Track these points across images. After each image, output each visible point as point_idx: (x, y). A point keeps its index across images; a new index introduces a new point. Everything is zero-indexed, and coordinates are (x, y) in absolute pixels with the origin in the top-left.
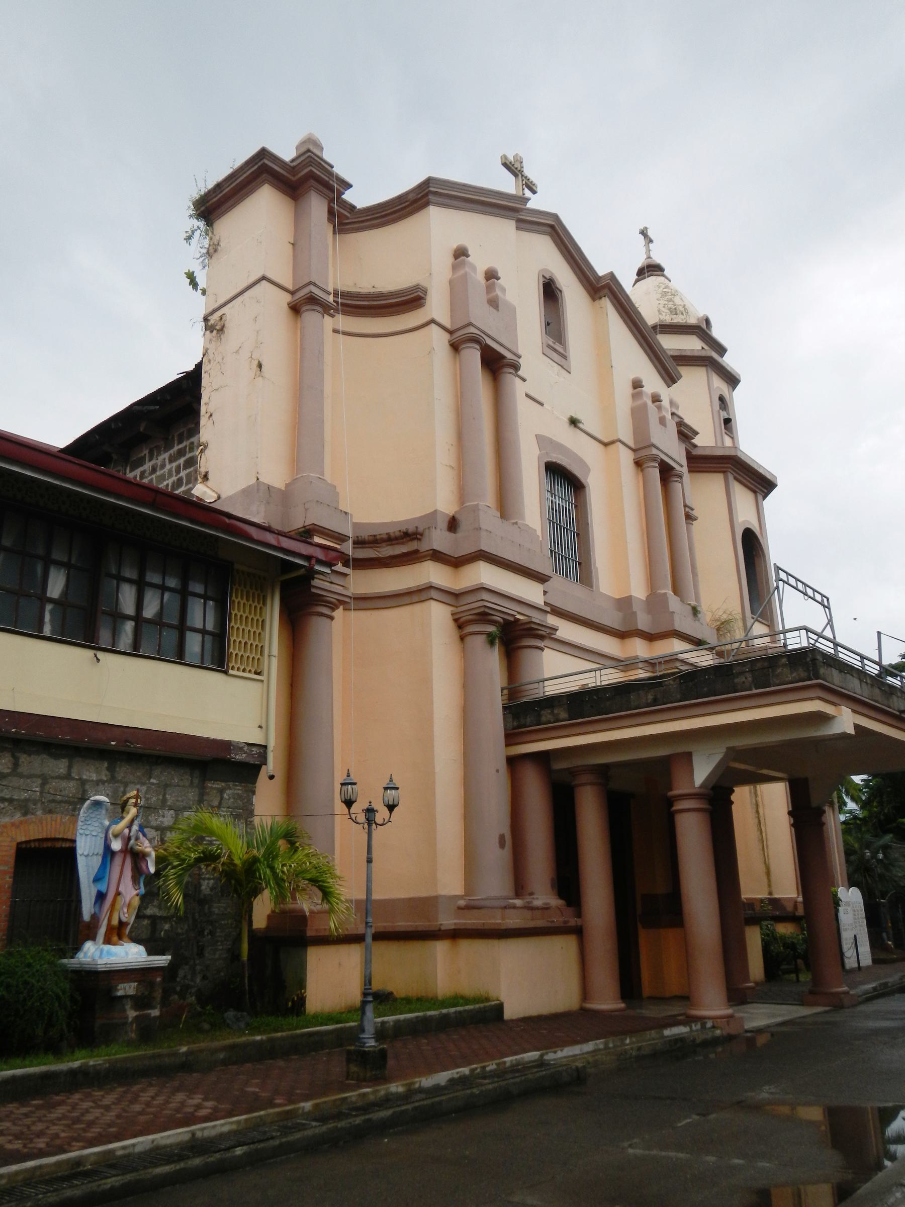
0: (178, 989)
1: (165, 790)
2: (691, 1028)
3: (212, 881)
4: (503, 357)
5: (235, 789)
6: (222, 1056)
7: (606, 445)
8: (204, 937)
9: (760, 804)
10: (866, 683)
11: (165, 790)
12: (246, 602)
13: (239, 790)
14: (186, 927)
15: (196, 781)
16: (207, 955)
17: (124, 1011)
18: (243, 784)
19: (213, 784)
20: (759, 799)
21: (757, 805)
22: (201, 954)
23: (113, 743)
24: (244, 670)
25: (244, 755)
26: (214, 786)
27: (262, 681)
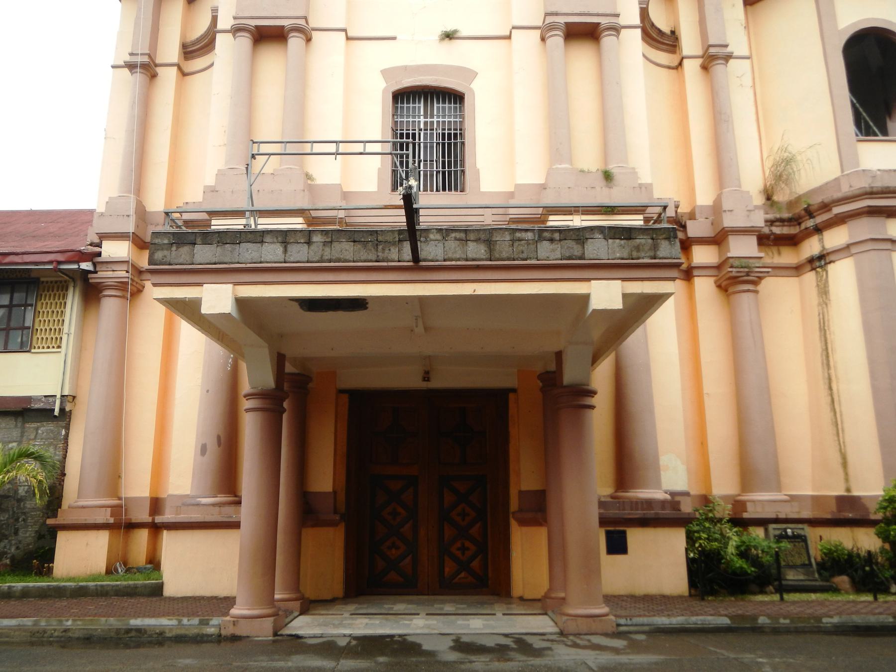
2: (180, 621)
3: (26, 487)
4: (283, 27)
5: (48, 426)
7: (509, 37)
9: (833, 378)
10: (309, 243)
12: (53, 302)
13: (51, 426)
15: (19, 424)
16: (20, 534)
18: (54, 423)
20: (832, 372)
21: (830, 379)
22: (16, 533)
24: (48, 347)
25: (42, 404)
27: (60, 352)
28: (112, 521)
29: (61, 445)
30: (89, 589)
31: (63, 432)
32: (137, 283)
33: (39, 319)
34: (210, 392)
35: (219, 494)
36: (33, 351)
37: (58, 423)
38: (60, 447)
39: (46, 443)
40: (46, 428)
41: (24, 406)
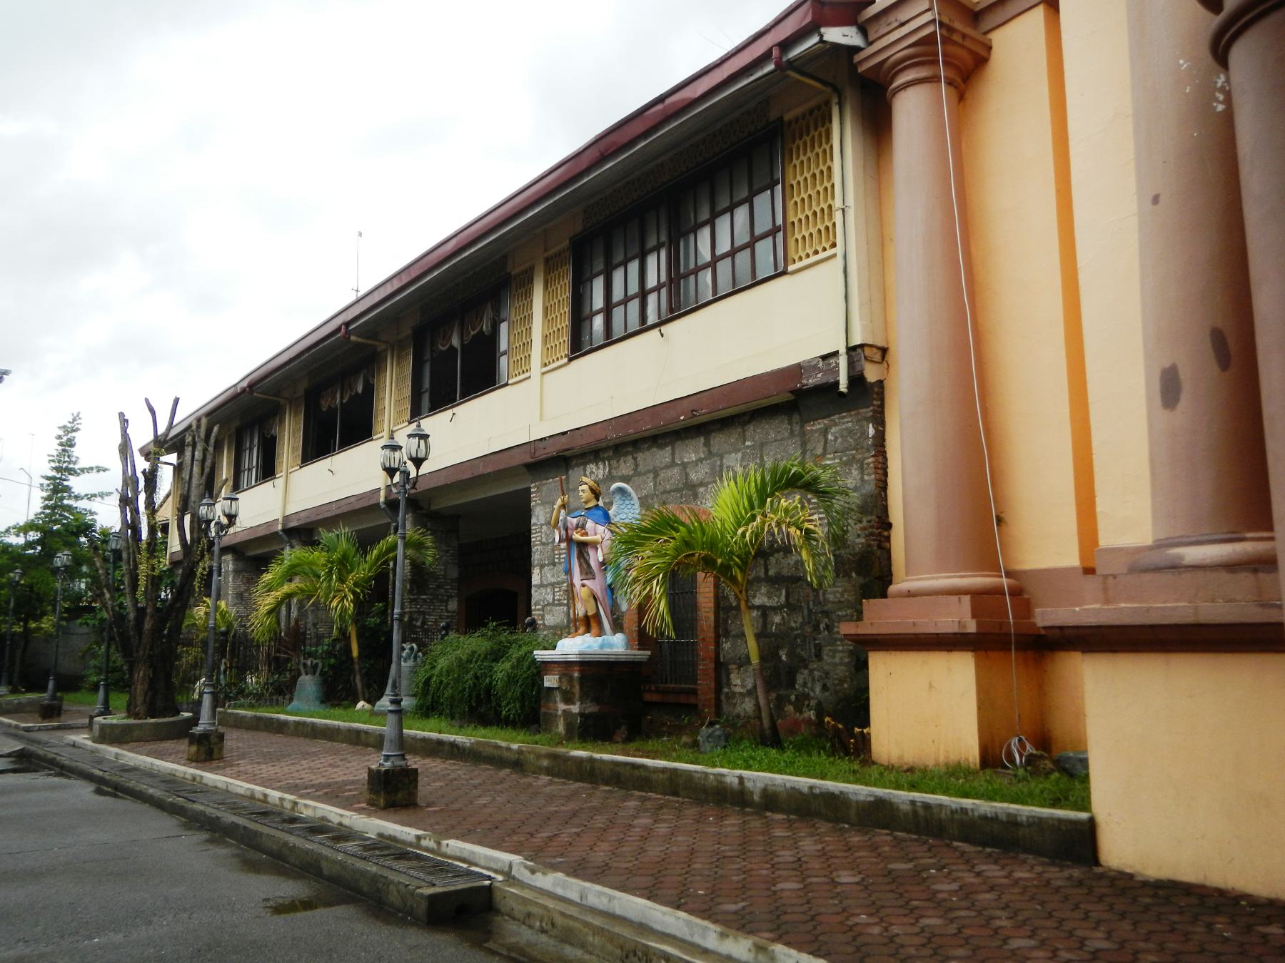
0: (793, 698)
1: (761, 450)
5: (843, 423)
6: (545, 763)
8: (820, 633)
11: (761, 450)
13: (847, 422)
14: (800, 620)
15: (797, 428)
16: (825, 657)
17: (556, 702)
18: (853, 413)
19: (813, 425)
22: (819, 656)
23: (682, 418)
24: (816, 252)
25: (819, 375)
26: (814, 428)
28: (972, 627)
29: (871, 460)
30: (898, 809)
31: (871, 431)
32: (964, 36)
33: (792, 202)
34: (1162, 198)
35: (1250, 530)
36: (791, 268)
37: (858, 414)
38: (868, 464)
39: (845, 459)
40: (839, 427)
41: (792, 386)
